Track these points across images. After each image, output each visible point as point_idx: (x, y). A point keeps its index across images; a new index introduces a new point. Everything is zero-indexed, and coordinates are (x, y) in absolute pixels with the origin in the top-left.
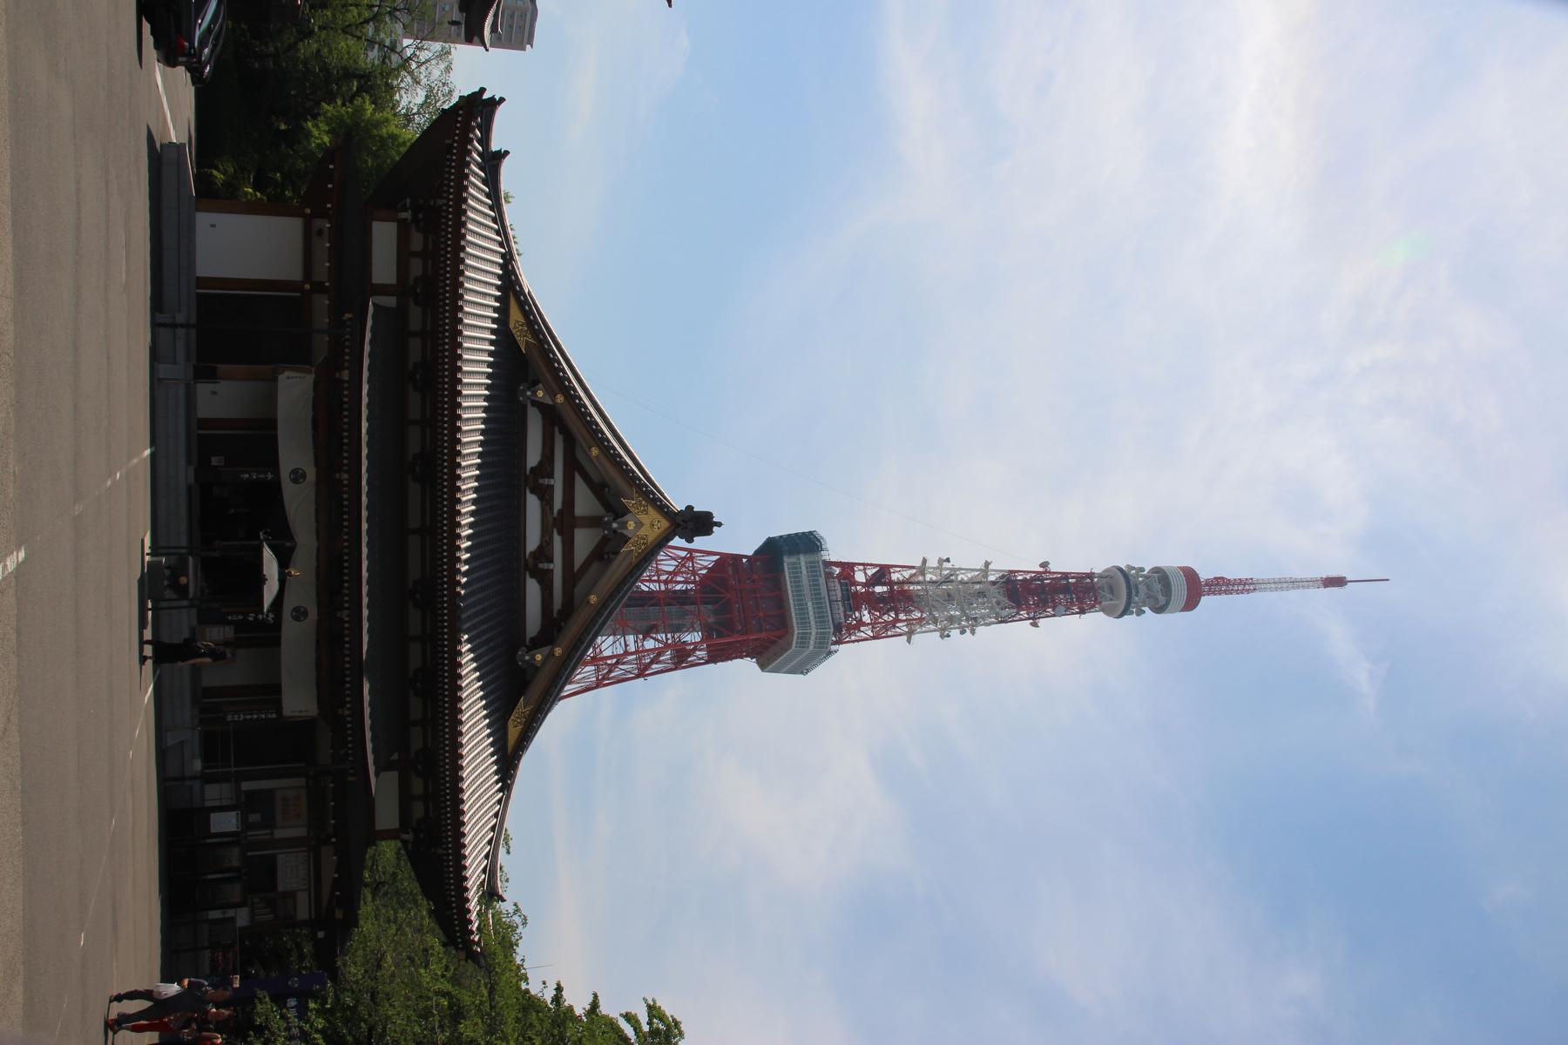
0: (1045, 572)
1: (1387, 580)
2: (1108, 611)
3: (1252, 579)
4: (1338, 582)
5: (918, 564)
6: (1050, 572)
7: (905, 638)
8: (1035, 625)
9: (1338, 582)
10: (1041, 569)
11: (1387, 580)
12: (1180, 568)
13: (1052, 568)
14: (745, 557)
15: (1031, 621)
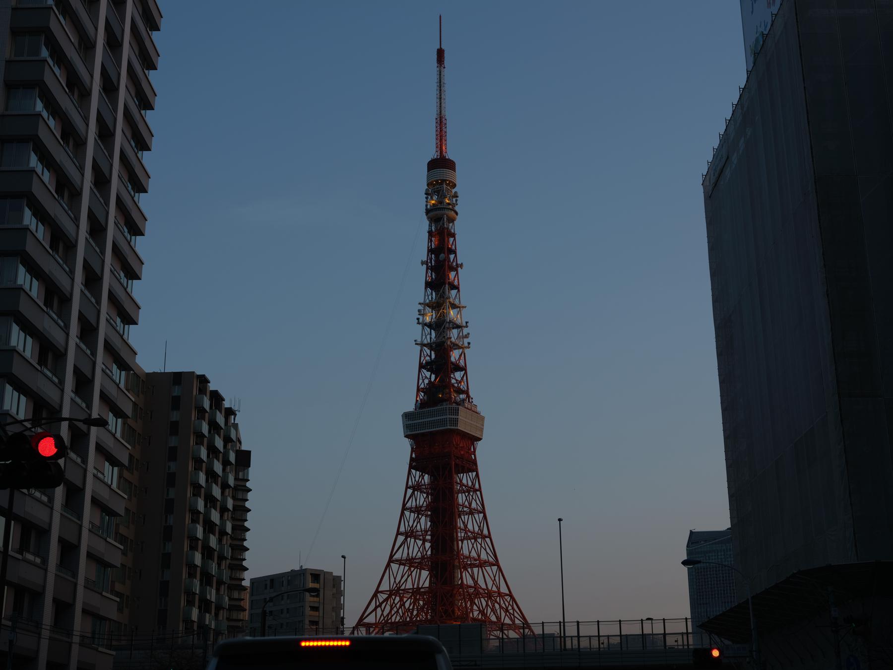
0: (427, 265)
1: (440, 16)
2: (452, 220)
3: (436, 119)
4: (440, 53)
5: (419, 347)
6: (427, 261)
7: (466, 351)
8: (461, 266)
9: (440, 53)
10: (425, 266)
11: (440, 16)
12: (428, 171)
13: (425, 259)
14: (411, 455)
15: (459, 269)
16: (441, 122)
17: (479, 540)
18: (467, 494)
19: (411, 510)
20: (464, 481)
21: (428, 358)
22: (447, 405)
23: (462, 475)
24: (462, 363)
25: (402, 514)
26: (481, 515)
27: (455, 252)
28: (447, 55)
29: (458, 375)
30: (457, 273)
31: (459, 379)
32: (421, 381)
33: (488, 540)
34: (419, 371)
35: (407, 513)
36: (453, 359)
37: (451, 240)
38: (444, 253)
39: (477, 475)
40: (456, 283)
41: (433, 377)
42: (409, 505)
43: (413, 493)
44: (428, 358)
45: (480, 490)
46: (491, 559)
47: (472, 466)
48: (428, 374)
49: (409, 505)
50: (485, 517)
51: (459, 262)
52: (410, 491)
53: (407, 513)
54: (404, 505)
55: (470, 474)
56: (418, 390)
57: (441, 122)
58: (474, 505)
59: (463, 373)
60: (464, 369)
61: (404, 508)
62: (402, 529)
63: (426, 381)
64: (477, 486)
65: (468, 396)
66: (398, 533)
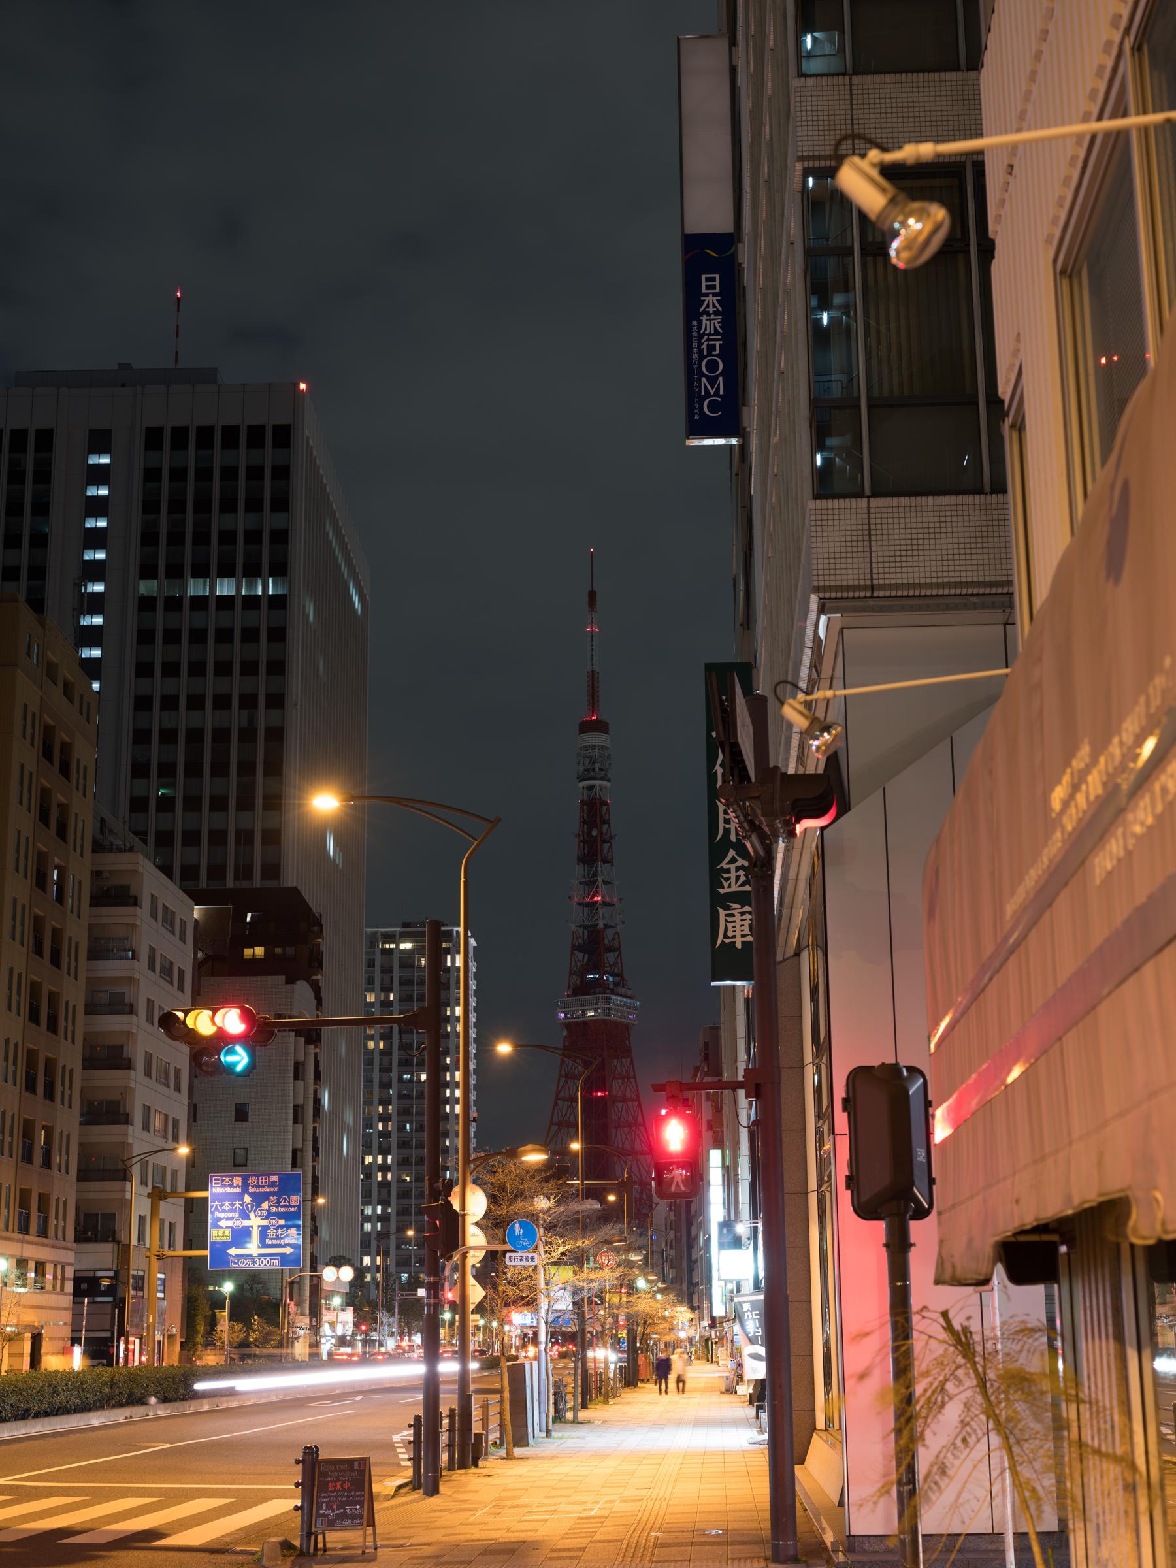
4: (592, 595)
9: (592, 595)
15: (613, 841)
16: (593, 676)
17: (634, 1128)
18: (620, 1081)
19: (564, 1099)
20: (619, 1068)
21: (580, 941)
22: (600, 993)
23: (616, 1061)
24: (616, 945)
25: (556, 1103)
26: (636, 1103)
27: (608, 822)
28: (598, 597)
29: (611, 957)
30: (610, 847)
31: (612, 962)
32: (573, 964)
33: (642, 1128)
34: (572, 953)
35: (560, 1103)
36: (606, 942)
38: (596, 827)
39: (632, 1062)
40: (609, 857)
41: (586, 956)
42: (562, 1095)
43: (566, 1081)
44: (580, 941)
45: (634, 1077)
46: (645, 1148)
47: (627, 1052)
48: (579, 955)
49: (562, 1095)
50: (639, 1104)
51: (613, 834)
52: (563, 1080)
53: (560, 1103)
54: (557, 1094)
55: (624, 1060)
56: (571, 974)
57: (593, 676)
58: (628, 1094)
59: (617, 953)
60: (618, 950)
61: (557, 1098)
62: (555, 1120)
63: (579, 964)
64: (631, 1073)
65: (622, 979)
66: (552, 1123)
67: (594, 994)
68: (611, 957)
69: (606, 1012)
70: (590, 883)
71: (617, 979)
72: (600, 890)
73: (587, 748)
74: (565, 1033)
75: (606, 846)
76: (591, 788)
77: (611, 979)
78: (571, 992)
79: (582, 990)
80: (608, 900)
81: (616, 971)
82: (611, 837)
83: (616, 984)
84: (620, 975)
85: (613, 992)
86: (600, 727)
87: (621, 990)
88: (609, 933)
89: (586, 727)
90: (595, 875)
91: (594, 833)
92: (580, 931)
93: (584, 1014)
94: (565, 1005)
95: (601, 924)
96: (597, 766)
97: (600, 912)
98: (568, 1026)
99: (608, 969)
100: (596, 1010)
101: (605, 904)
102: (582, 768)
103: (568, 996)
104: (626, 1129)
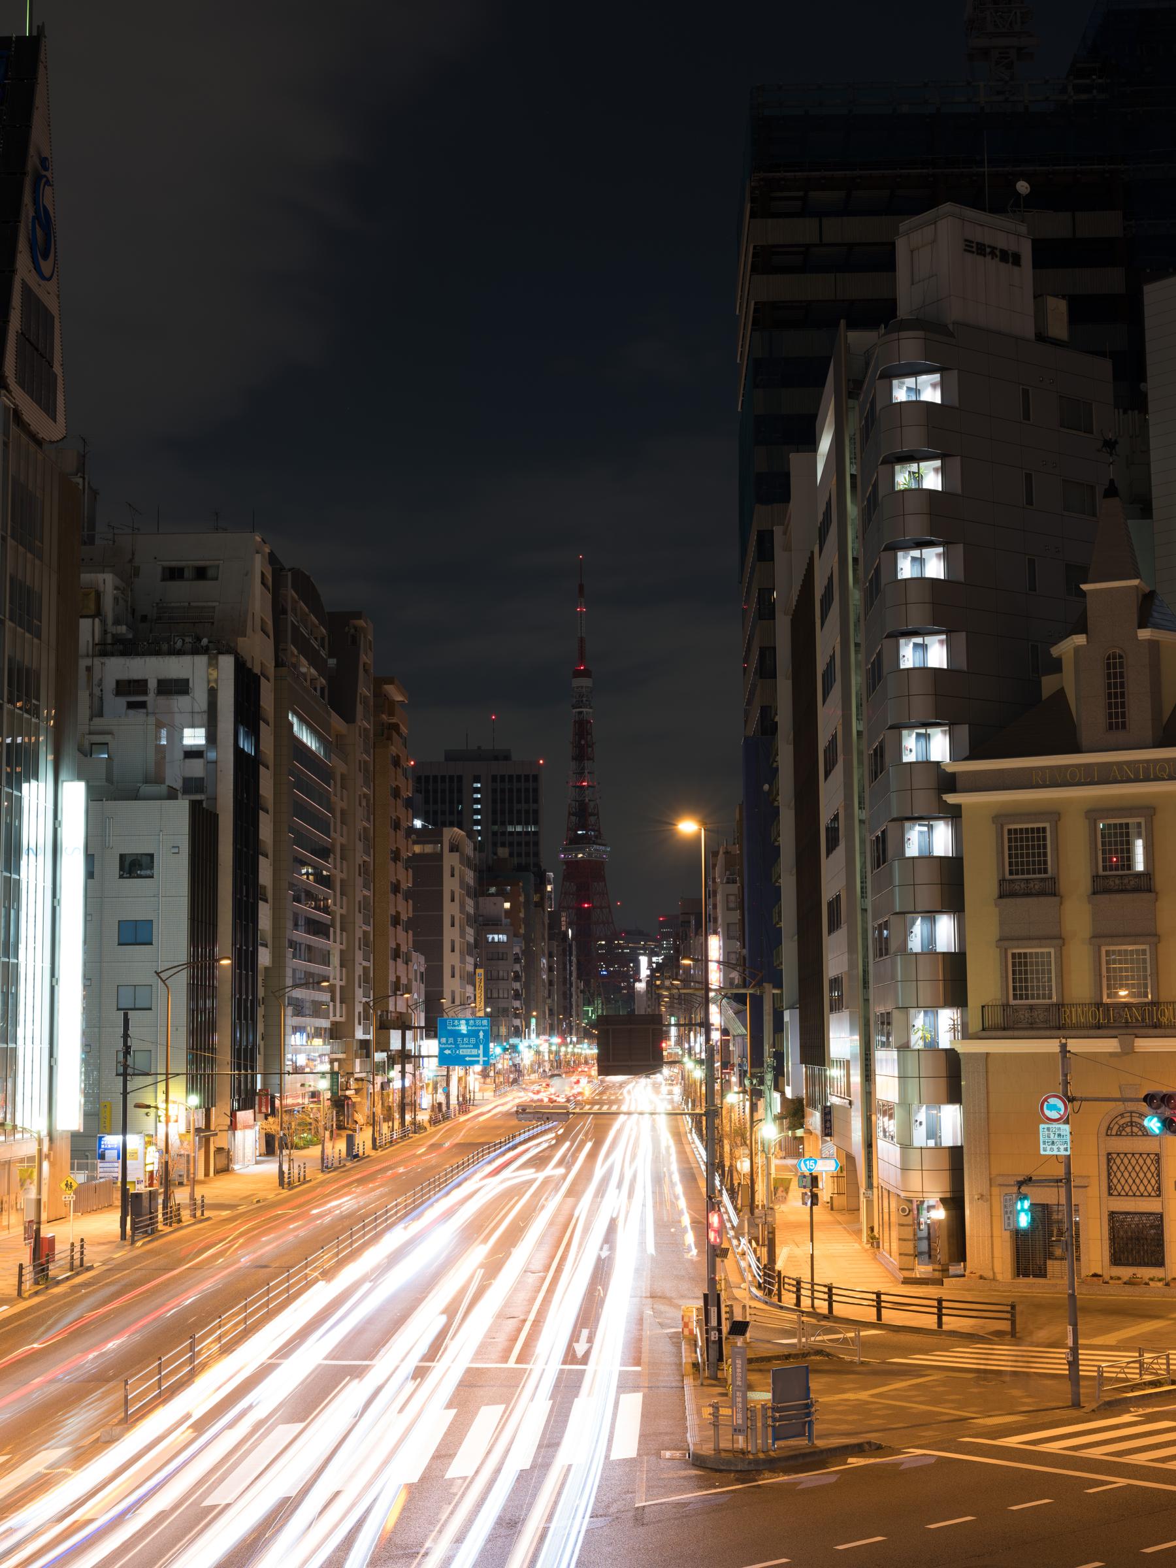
4: (581, 587)
9: (581, 587)
16: (582, 640)
23: (596, 884)
26: (607, 910)
27: (591, 734)
34: (569, 817)
37: (589, 725)
39: (605, 885)
44: (574, 810)
48: (573, 818)
50: (610, 911)
57: (582, 640)
60: (597, 814)
65: (600, 833)
67: (583, 844)
68: (592, 819)
69: (590, 854)
70: (580, 774)
71: (597, 833)
72: (586, 778)
73: (578, 687)
74: (564, 867)
75: (590, 749)
76: (581, 713)
77: (593, 833)
78: (568, 842)
79: (576, 842)
80: (591, 784)
81: (596, 828)
82: (593, 744)
83: (596, 837)
84: (599, 831)
85: (594, 843)
86: (586, 674)
87: (599, 841)
88: (592, 804)
89: (578, 674)
90: (583, 768)
91: (583, 742)
92: (574, 803)
93: (576, 856)
94: (565, 851)
95: (587, 801)
96: (584, 699)
97: (587, 792)
98: (568, 863)
99: (590, 827)
100: (584, 854)
101: (589, 786)
102: (575, 700)
103: (566, 844)
104: (602, 925)
